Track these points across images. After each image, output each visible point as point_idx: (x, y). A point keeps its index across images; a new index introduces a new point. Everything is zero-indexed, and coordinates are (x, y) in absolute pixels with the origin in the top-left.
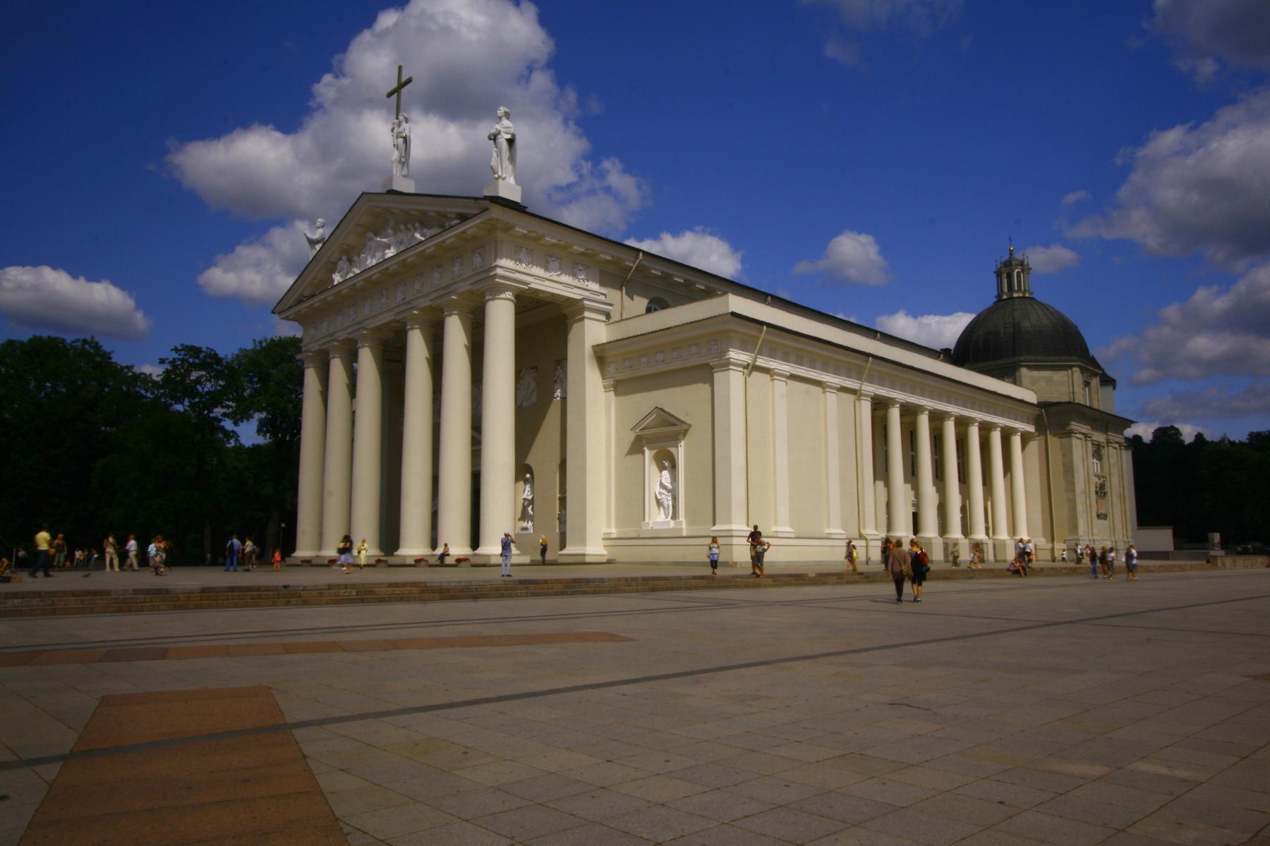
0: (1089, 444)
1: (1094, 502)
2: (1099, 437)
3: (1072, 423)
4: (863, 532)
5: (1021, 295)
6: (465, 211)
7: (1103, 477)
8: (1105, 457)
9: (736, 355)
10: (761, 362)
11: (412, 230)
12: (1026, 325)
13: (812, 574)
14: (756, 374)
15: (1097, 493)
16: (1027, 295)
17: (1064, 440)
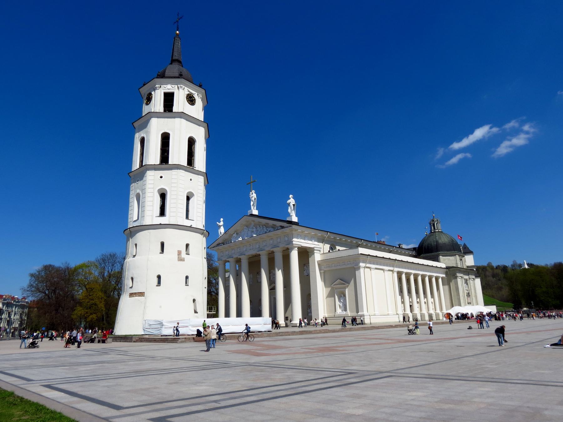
0: (463, 280)
1: (466, 299)
2: (466, 277)
3: (457, 274)
4: (397, 312)
5: (438, 231)
6: (283, 225)
7: (469, 290)
8: (469, 284)
9: (362, 265)
10: (368, 265)
11: (262, 228)
12: (440, 241)
13: (394, 325)
14: (366, 269)
15: (467, 296)
16: (440, 231)
17: (455, 280)
